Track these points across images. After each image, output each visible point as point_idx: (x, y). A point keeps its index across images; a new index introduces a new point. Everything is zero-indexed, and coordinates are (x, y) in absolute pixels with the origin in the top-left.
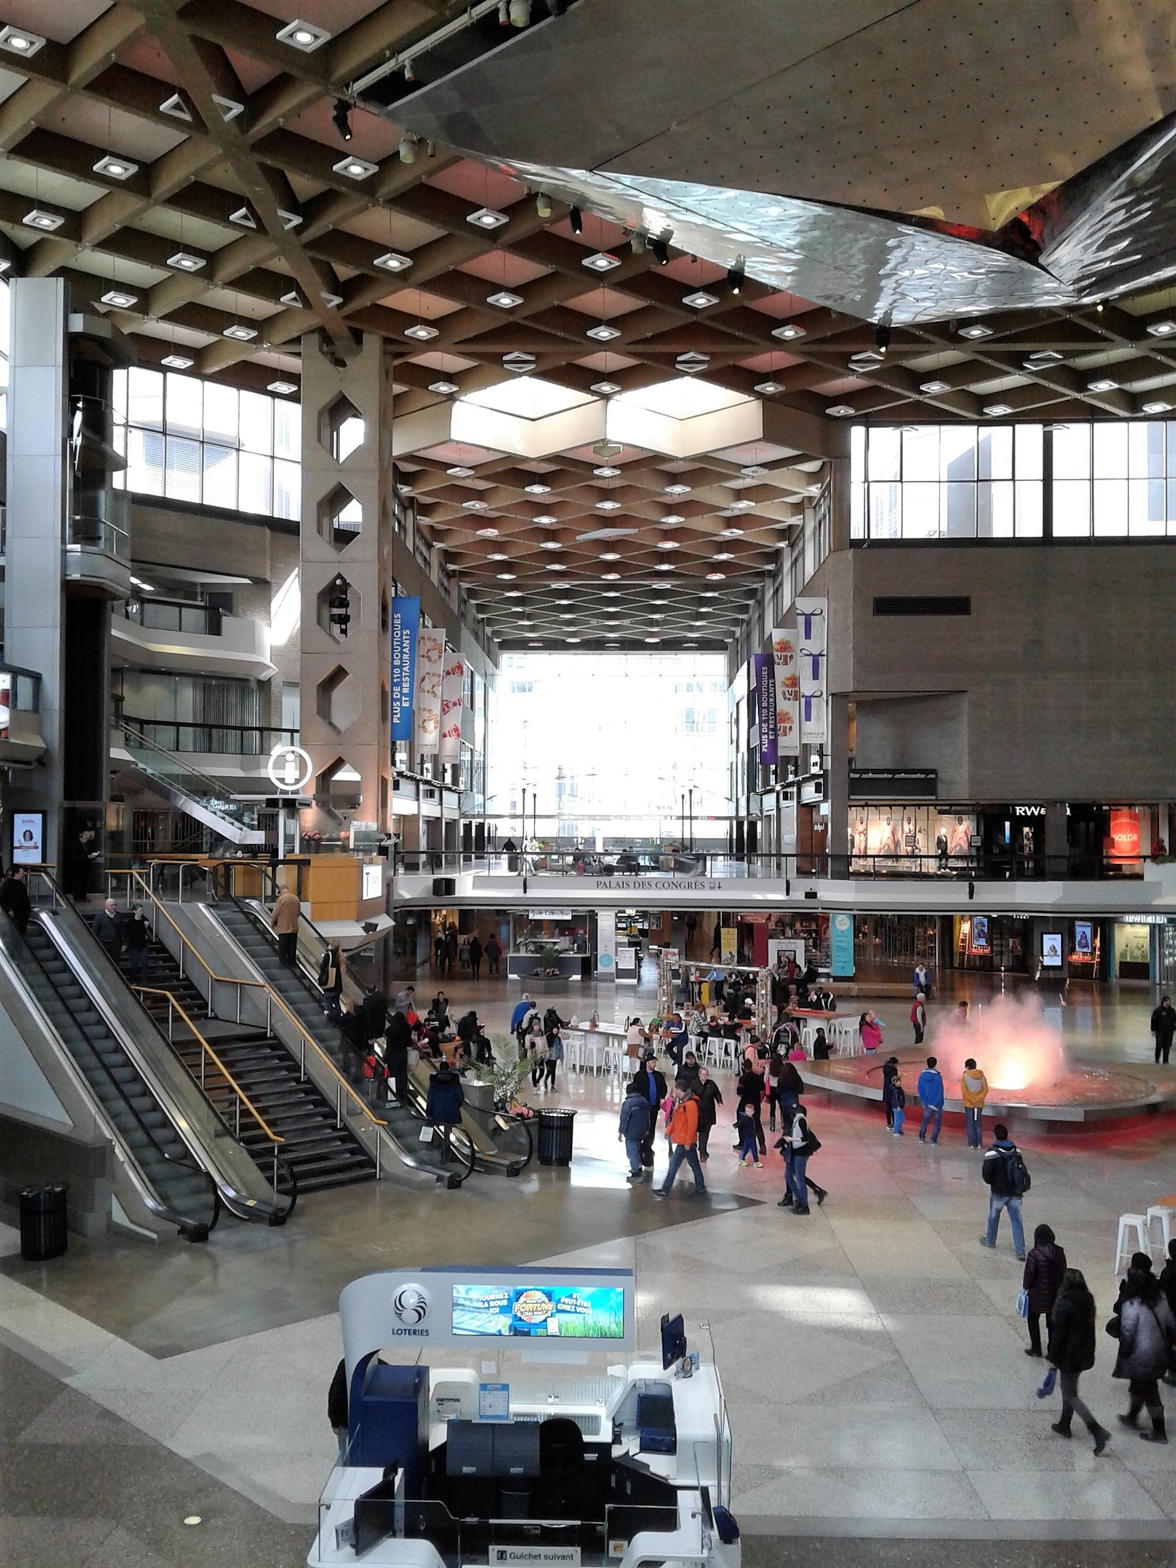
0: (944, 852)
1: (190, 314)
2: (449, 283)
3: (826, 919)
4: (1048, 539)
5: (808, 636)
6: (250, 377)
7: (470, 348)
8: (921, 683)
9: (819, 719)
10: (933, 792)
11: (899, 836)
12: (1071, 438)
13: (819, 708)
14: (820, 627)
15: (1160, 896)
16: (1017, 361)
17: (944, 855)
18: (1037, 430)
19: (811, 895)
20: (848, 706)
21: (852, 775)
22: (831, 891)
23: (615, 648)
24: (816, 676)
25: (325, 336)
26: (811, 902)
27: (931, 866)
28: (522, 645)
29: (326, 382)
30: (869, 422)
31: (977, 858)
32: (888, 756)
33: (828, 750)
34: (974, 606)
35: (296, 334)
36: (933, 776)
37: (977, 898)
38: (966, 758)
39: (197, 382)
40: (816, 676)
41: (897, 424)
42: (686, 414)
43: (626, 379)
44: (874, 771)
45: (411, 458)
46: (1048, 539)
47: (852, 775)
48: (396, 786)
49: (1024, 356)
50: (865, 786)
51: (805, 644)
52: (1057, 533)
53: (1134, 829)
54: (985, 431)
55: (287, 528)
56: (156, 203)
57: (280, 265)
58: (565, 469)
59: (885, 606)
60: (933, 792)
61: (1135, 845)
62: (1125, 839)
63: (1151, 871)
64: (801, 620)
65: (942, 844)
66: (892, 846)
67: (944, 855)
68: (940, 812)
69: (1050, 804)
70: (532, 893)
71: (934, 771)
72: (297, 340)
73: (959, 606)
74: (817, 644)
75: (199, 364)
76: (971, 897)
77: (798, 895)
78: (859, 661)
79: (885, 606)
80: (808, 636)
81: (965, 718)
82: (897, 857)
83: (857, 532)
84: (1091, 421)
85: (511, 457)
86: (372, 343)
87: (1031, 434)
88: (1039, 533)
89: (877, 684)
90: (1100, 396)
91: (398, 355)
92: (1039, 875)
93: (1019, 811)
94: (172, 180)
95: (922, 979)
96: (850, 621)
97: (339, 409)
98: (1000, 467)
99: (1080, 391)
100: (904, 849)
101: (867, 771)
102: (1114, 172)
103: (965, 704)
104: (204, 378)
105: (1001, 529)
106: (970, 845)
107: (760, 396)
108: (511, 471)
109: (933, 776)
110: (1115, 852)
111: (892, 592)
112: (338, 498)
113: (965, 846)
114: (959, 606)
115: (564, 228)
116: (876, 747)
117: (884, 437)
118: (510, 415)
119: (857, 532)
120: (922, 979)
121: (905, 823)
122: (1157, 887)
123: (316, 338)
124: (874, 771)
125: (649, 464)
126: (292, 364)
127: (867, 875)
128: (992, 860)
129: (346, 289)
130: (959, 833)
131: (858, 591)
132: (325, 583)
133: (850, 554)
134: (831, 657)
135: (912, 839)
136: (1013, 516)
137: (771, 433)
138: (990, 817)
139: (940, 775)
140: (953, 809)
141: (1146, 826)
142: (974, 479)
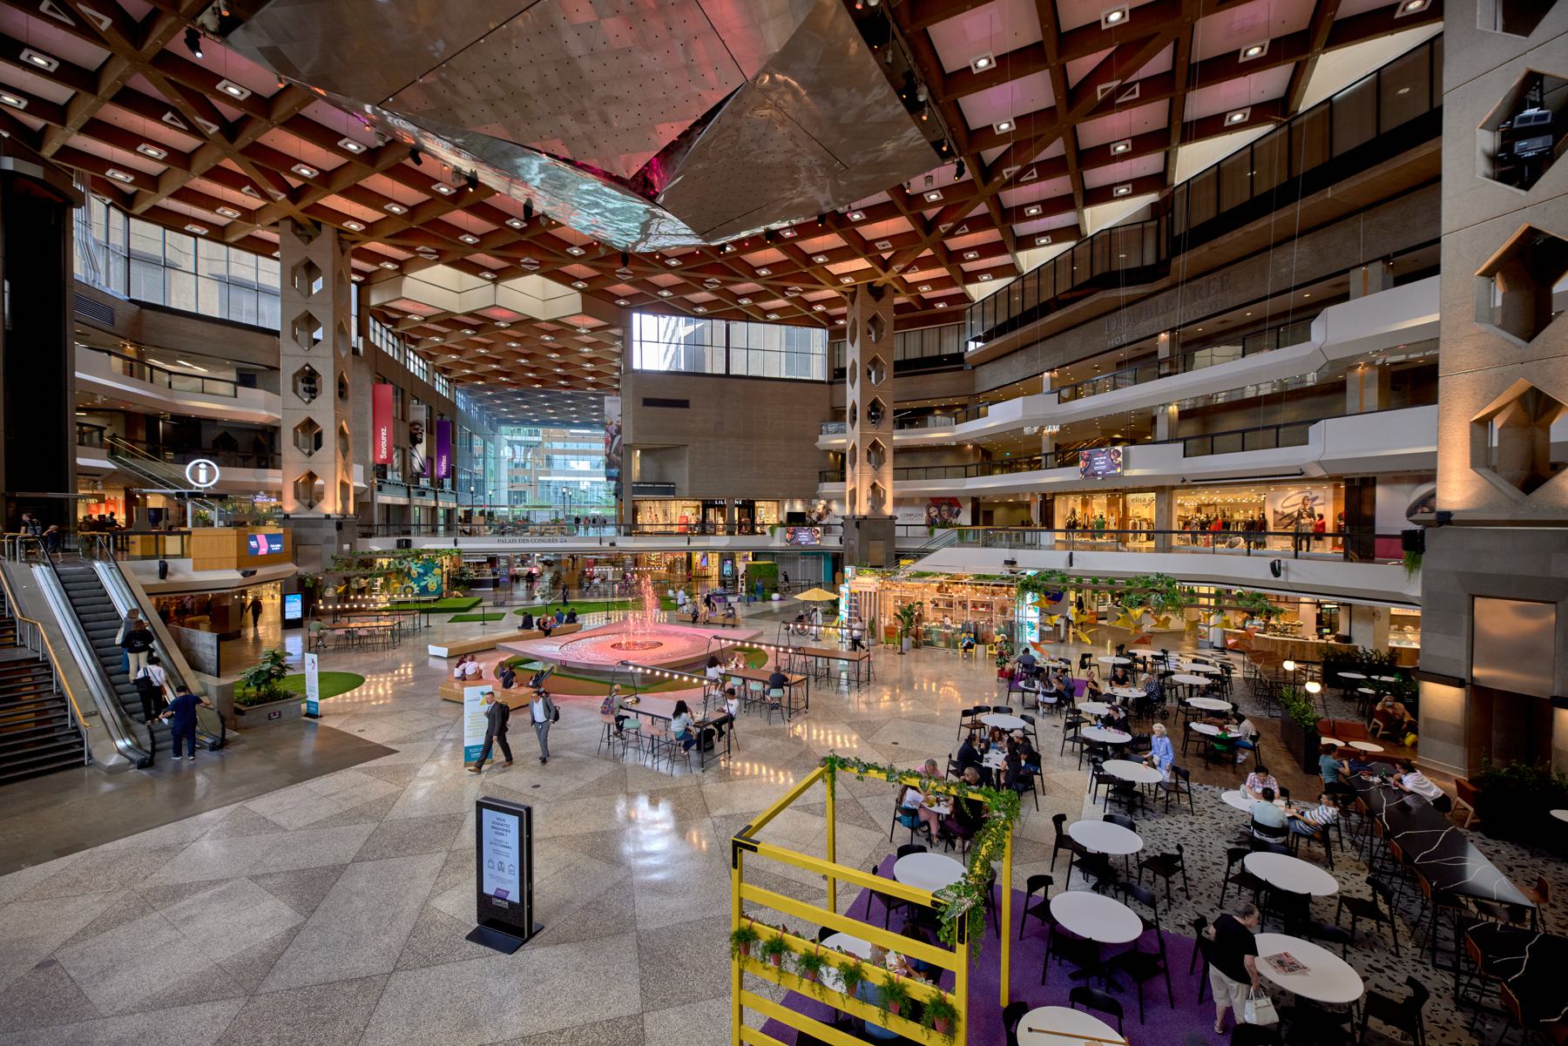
1: (184, 194)
2: (357, 193)
4: (727, 375)
6: (262, 248)
7: (400, 242)
8: (666, 441)
12: (738, 328)
18: (723, 323)
25: (297, 226)
28: (508, 422)
29: (300, 251)
30: (642, 310)
35: (275, 220)
39: (224, 248)
41: (655, 314)
42: (533, 295)
43: (500, 276)
45: (382, 306)
46: (727, 375)
48: (380, 489)
54: (700, 324)
55: (275, 333)
56: (103, 101)
57: (230, 164)
58: (482, 322)
59: (648, 402)
70: (460, 546)
72: (275, 224)
73: (684, 404)
75: (218, 234)
78: (635, 429)
79: (648, 402)
83: (636, 366)
85: (447, 312)
86: (328, 231)
87: (720, 325)
90: (746, 307)
91: (354, 242)
94: (109, 83)
97: (311, 270)
103: (687, 450)
104: (228, 245)
105: (708, 371)
107: (580, 290)
108: (449, 321)
112: (309, 322)
114: (684, 404)
115: (409, 162)
118: (436, 287)
119: (636, 366)
123: (289, 223)
125: (526, 323)
126: (274, 237)
129: (295, 195)
132: (298, 368)
137: (587, 310)
142: (693, 342)
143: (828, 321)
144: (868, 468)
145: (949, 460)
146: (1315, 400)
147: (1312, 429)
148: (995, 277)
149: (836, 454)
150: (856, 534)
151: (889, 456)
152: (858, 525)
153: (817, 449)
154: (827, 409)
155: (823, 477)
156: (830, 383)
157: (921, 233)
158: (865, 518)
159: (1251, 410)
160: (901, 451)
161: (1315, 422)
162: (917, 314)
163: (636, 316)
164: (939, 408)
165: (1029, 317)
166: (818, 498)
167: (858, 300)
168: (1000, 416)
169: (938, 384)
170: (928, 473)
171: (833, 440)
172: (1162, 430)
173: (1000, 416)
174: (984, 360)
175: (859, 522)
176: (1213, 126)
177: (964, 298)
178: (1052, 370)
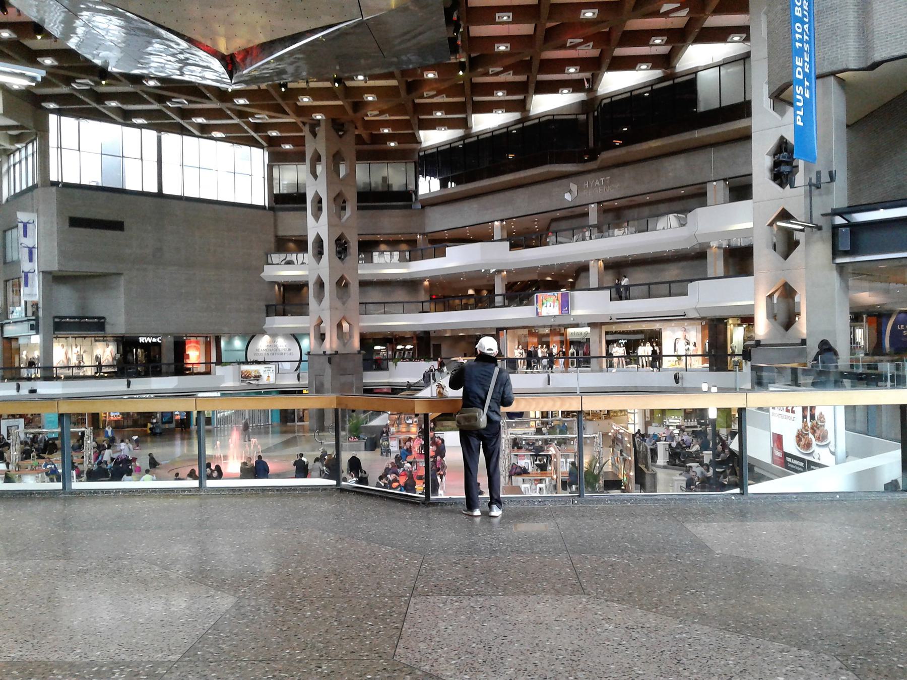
0: (100, 363)
5: (25, 235)
9: (33, 286)
11: (69, 355)
13: (33, 280)
14: (33, 230)
15: (223, 382)
16: (161, 99)
17: (99, 367)
19: (33, 391)
20: (54, 279)
22: (45, 389)
24: (31, 260)
26: (33, 395)
27: (90, 372)
30: (60, 112)
31: (117, 365)
32: (73, 309)
33: (40, 305)
34: (126, 225)
40: (31, 260)
44: (70, 318)
46: (160, 194)
47: (57, 320)
49: (169, 99)
50: (62, 326)
51: (23, 240)
52: (164, 192)
53: (197, 349)
59: (75, 222)
61: (199, 357)
62: (194, 355)
63: (218, 370)
64: (21, 226)
65: (97, 358)
66: (65, 361)
67: (99, 367)
68: (96, 341)
69: (165, 335)
71: (103, 318)
73: (117, 226)
74: (32, 240)
77: (24, 391)
78: (63, 254)
79: (75, 222)
80: (25, 235)
81: (122, 289)
82: (69, 367)
83: (53, 177)
87: (150, 135)
89: (73, 267)
92: (157, 373)
93: (141, 340)
95: (110, 434)
96: (55, 229)
98: (132, 150)
99: (182, 119)
100: (74, 361)
101: (66, 317)
102: (287, 44)
103: (122, 280)
105: (132, 185)
106: (114, 359)
110: (188, 361)
111: (79, 214)
113: (111, 360)
114: (117, 226)
116: (67, 303)
117: (69, 123)
120: (110, 434)
121: (74, 347)
122: (222, 378)
127: (68, 378)
128: (125, 367)
130: (107, 352)
131: (60, 212)
133: (54, 189)
134: (42, 250)
135: (80, 358)
136: (138, 178)
138: (126, 344)
139: (107, 320)
140: (104, 339)
141: (203, 348)
143: (272, 144)
144: (339, 304)
145: (400, 295)
146: (690, 263)
147: (690, 286)
148: (450, 127)
149: (279, 284)
151: (354, 288)
152: (330, 361)
153: (262, 281)
154: (273, 239)
155: (273, 310)
156: (271, 208)
157: (403, 93)
158: (336, 353)
159: (650, 267)
160: (365, 284)
161: (691, 281)
162: (365, 147)
163: (53, 118)
164: (387, 242)
165: (468, 163)
166: (263, 333)
167: (321, 131)
168: (457, 259)
169: (389, 221)
170: (385, 306)
171: (284, 270)
172: (593, 278)
173: (457, 259)
174: (433, 202)
175: (331, 358)
176: (628, 64)
177: (416, 140)
178: (502, 220)
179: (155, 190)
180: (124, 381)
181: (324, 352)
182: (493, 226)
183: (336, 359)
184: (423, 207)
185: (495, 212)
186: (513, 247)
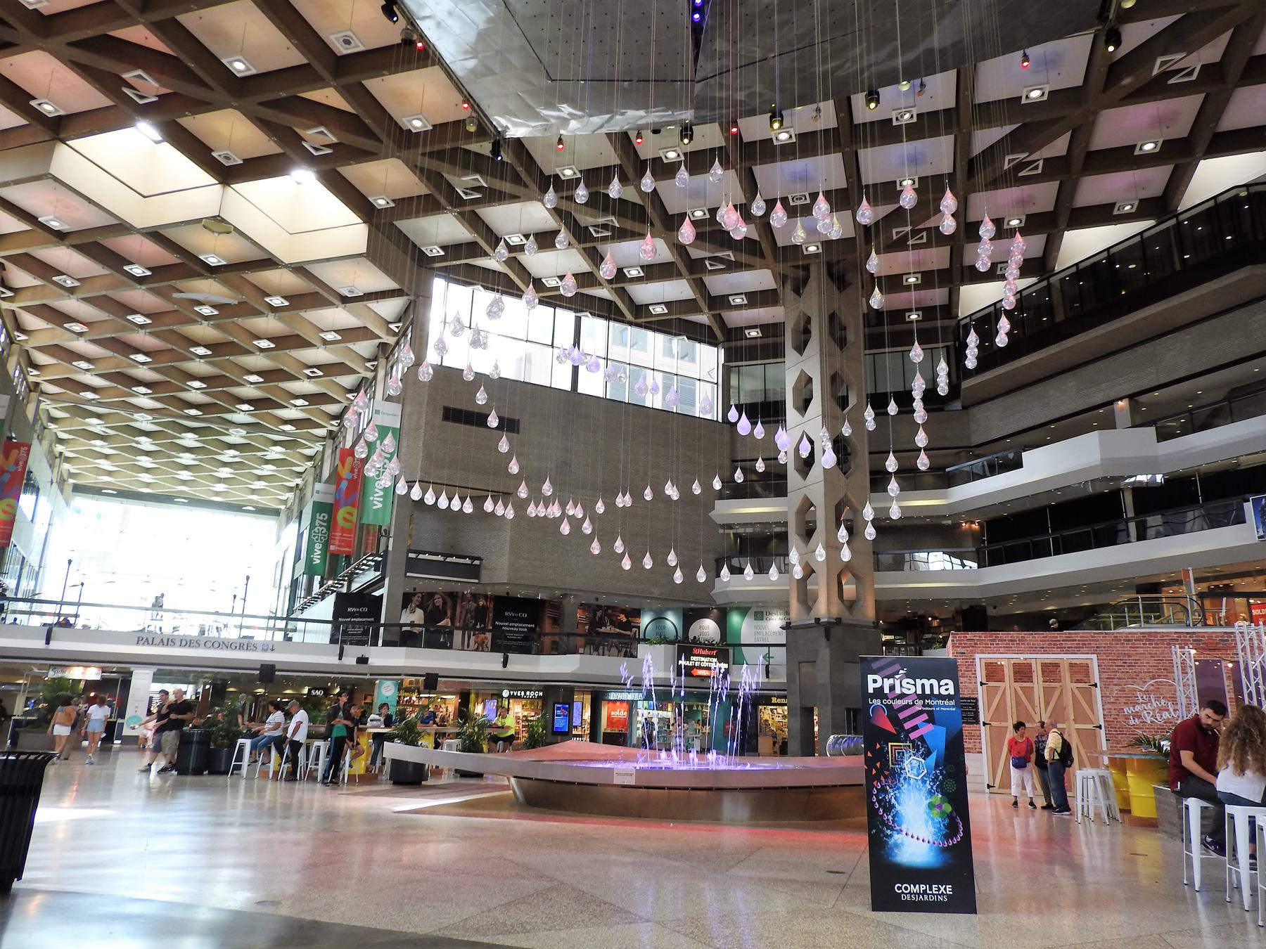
3: (372, 684)
10: (477, 576)
19: (363, 660)
21: (411, 555)
23: (184, 504)
26: (362, 668)
36: (477, 562)
37: (510, 668)
38: (507, 548)
47: (411, 555)
60: (477, 576)
71: (479, 559)
76: (505, 666)
77: (350, 661)
78: (428, 456)
84: (608, 318)
88: (568, 388)
96: (423, 422)
109: (477, 562)
124: (430, 554)
150: (825, 653)
153: (711, 523)
158: (839, 621)
168: (1045, 467)
175: (828, 629)
179: (567, 387)
180: (499, 657)
181: (817, 620)
182: (1113, 411)
183: (837, 631)
184: (965, 408)
185: (1114, 382)
186: (1163, 436)
